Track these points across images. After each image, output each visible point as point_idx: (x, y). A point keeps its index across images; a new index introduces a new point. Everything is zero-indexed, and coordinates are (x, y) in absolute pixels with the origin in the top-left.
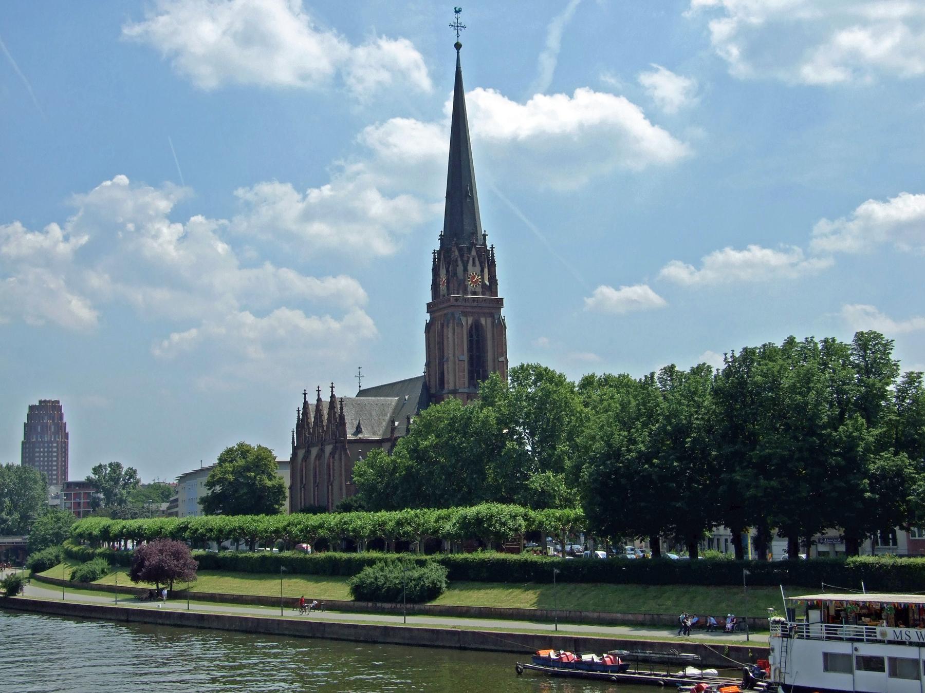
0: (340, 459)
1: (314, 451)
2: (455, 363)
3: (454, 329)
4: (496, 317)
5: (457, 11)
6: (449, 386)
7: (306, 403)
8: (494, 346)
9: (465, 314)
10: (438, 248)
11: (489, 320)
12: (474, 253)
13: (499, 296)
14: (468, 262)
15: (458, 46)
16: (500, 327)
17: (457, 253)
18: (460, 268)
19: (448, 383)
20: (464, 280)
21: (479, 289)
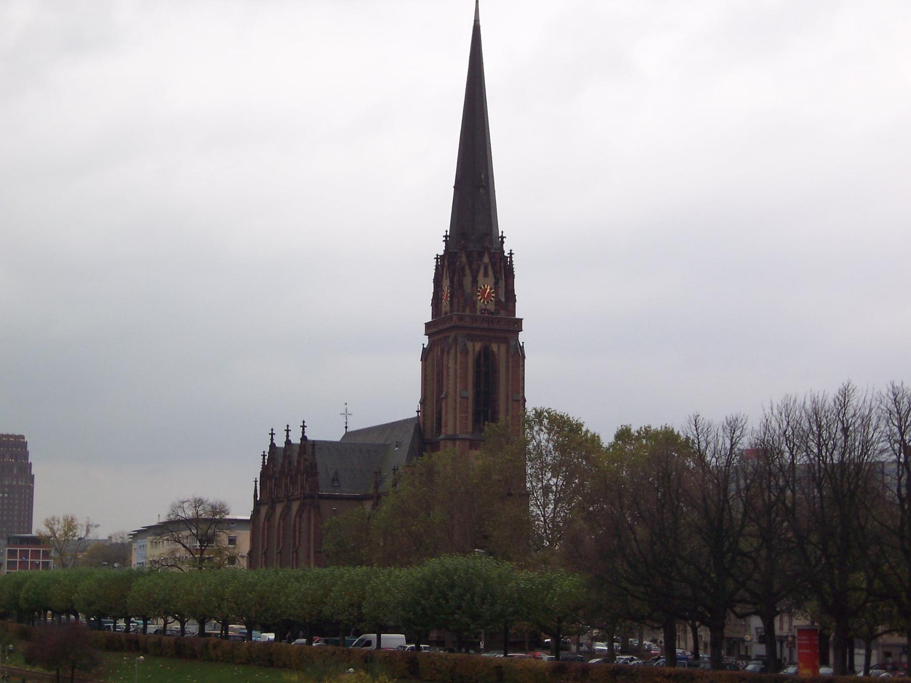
0: (309, 519)
1: (279, 509)
4: (512, 343)
6: (448, 429)
7: (272, 446)
9: (472, 338)
10: (442, 253)
11: (503, 348)
12: (486, 259)
13: (517, 316)
14: (478, 271)
16: (518, 355)
17: (464, 259)
18: (468, 280)
19: (446, 426)
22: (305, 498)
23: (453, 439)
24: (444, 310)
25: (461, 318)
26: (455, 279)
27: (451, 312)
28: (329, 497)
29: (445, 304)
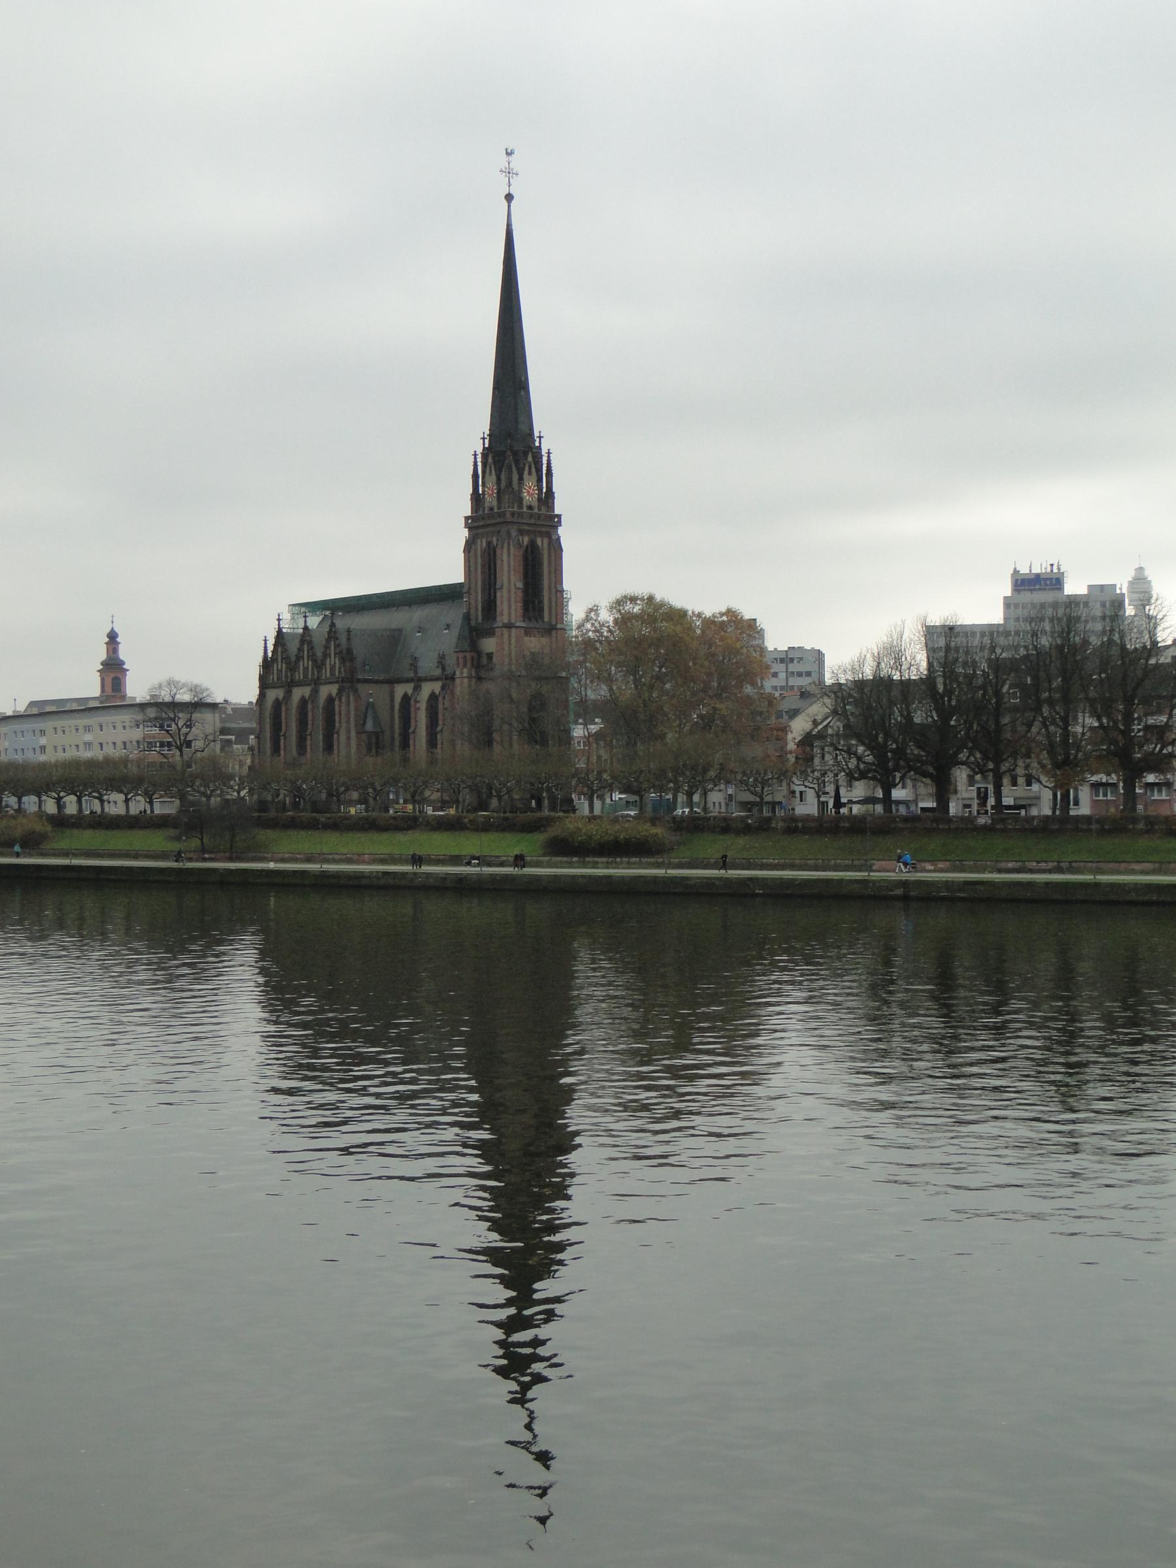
2: (509, 591)
3: (509, 549)
4: (554, 537)
5: (509, 153)
6: (503, 618)
8: (550, 572)
9: (521, 532)
10: (480, 450)
11: (546, 541)
12: (530, 459)
13: (556, 512)
15: (509, 198)
16: (556, 549)
18: (515, 477)
19: (502, 614)
20: (520, 491)
21: (535, 504)
22: (343, 681)
23: (509, 626)
24: (487, 505)
25: (513, 515)
26: (503, 477)
27: (499, 508)
28: (366, 681)
29: (490, 500)
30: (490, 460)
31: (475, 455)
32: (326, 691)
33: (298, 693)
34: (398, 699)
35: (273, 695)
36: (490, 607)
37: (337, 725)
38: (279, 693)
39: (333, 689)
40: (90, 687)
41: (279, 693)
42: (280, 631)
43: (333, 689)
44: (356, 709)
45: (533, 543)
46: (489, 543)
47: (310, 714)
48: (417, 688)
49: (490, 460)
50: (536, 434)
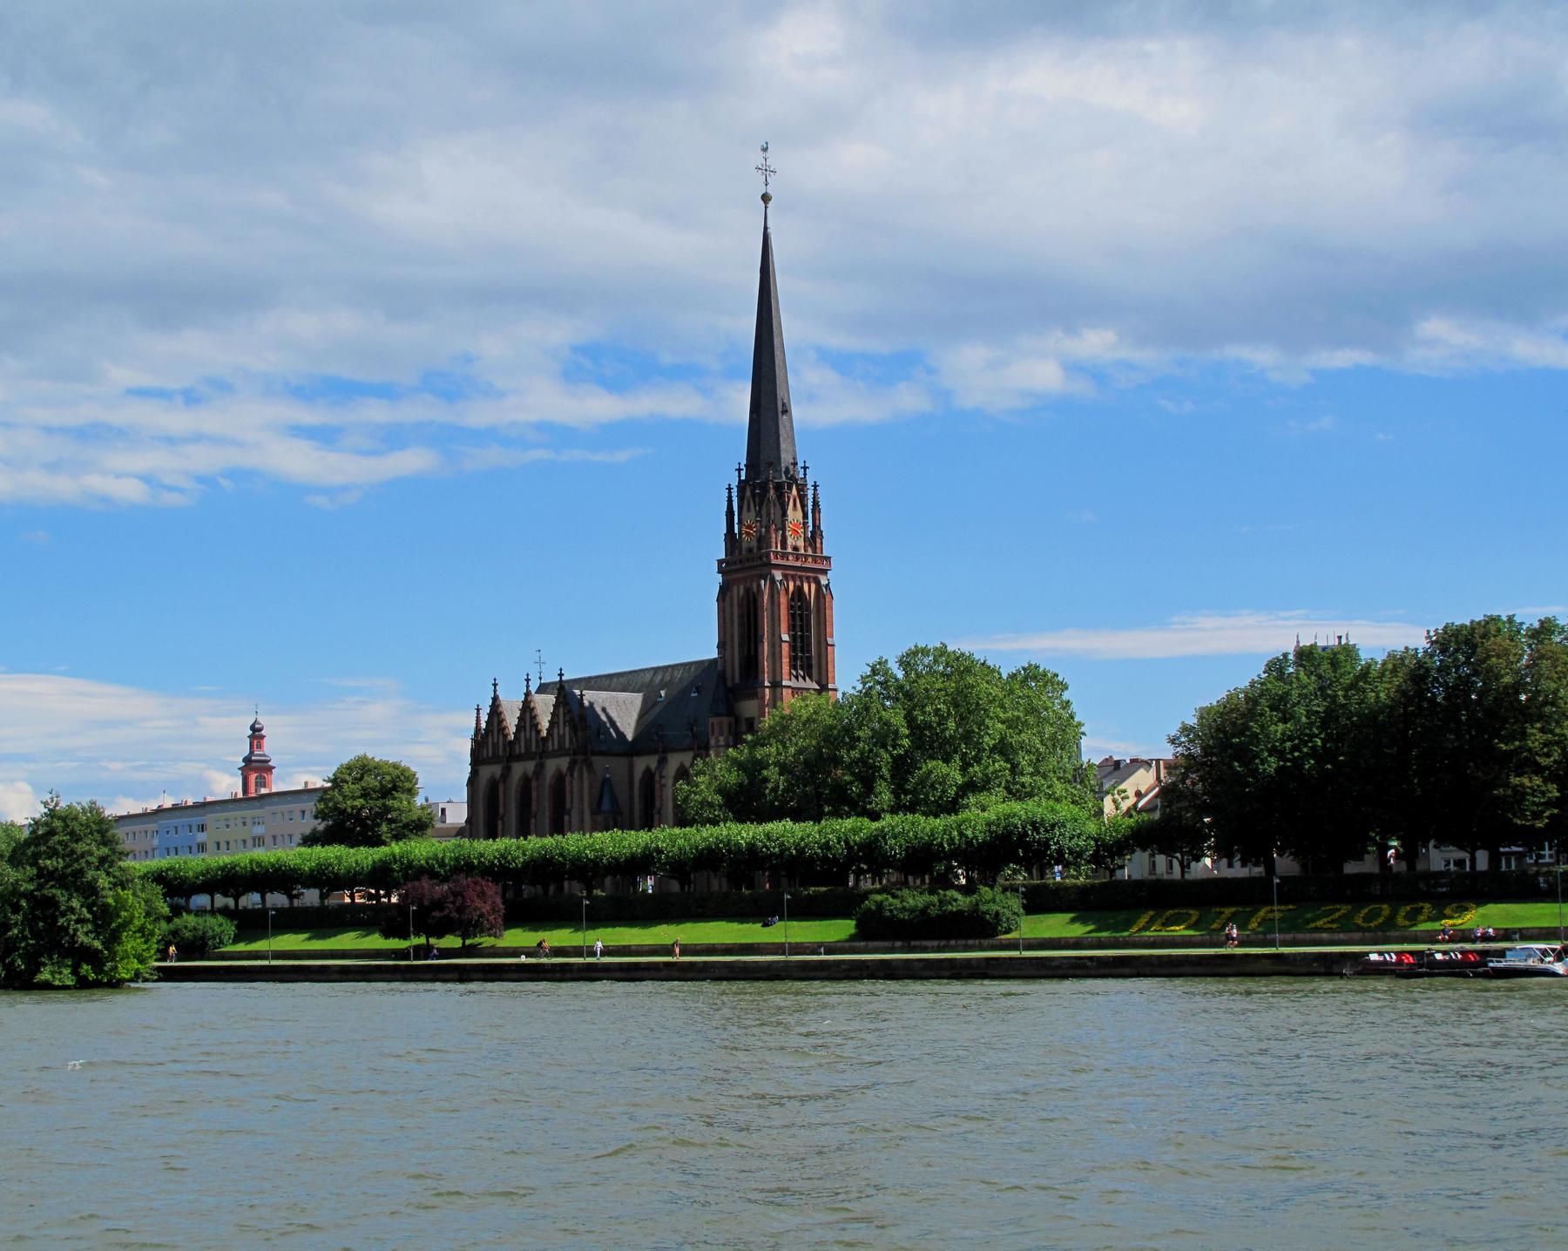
5: (765, 150)
11: (813, 586)
15: (766, 198)
16: (823, 594)
21: (801, 543)
24: (745, 546)
27: (759, 548)
30: (748, 493)
31: (730, 489)
32: (553, 765)
33: (519, 769)
34: (638, 775)
35: (487, 772)
36: (751, 664)
37: (568, 805)
38: (496, 770)
39: (564, 763)
40: (227, 785)
41: (496, 770)
42: (495, 699)
43: (564, 763)
44: (591, 787)
45: (799, 590)
46: (748, 591)
47: (534, 794)
48: (662, 762)
49: (748, 493)
50: (800, 464)
